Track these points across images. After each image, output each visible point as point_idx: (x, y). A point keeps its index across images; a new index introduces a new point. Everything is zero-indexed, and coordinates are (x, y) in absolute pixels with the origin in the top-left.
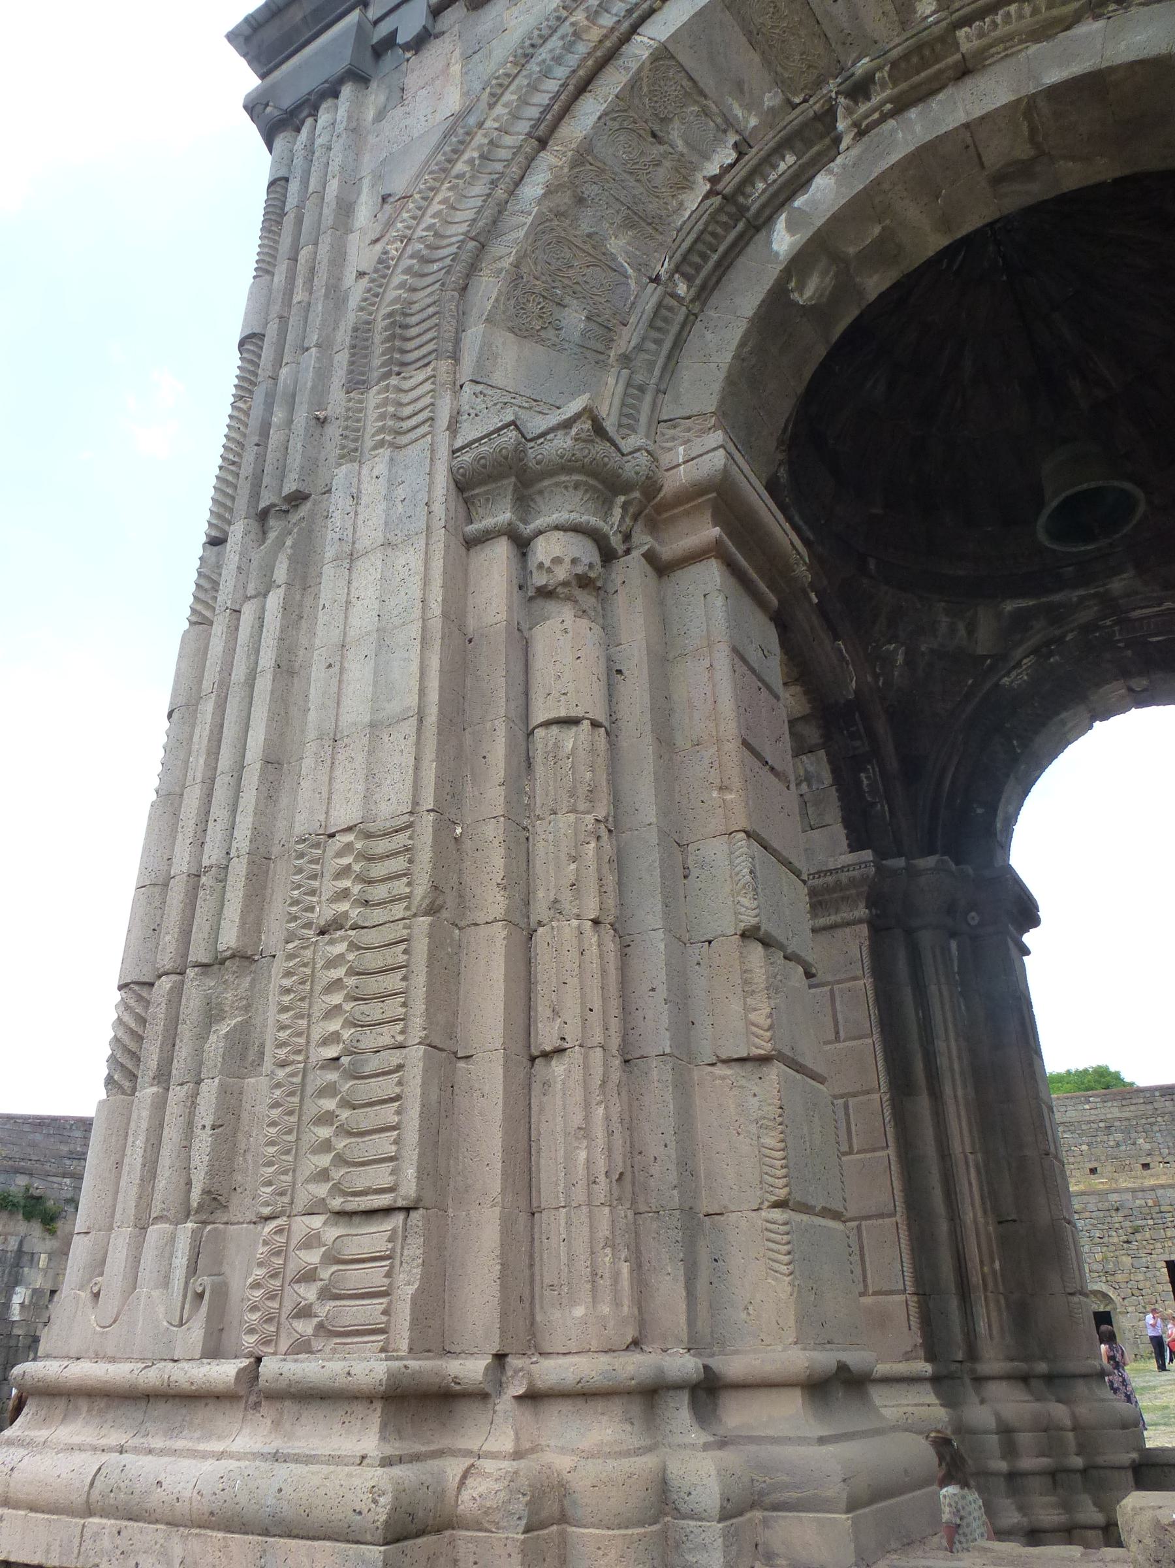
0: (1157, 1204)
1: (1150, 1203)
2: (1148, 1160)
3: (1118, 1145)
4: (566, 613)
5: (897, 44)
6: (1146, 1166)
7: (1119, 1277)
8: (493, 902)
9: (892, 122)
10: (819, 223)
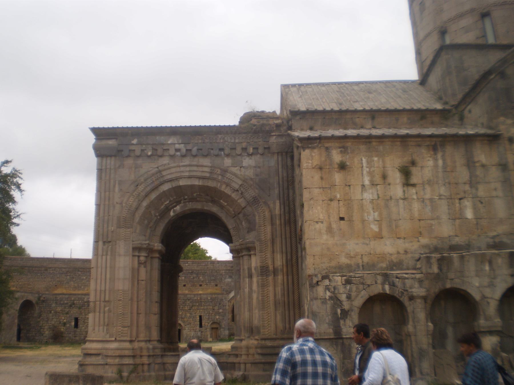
0: (201, 299)
1: (199, 299)
2: (202, 283)
3: (194, 278)
4: (143, 266)
6: (201, 285)
7: (185, 319)
8: (135, 299)
9: (187, 203)
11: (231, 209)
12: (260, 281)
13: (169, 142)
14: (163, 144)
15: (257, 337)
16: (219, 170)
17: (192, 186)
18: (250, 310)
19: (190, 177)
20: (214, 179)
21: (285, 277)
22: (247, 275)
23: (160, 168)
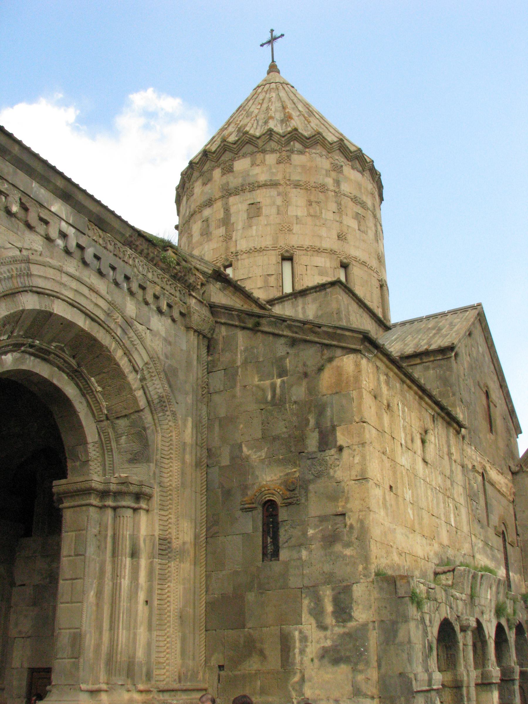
5: (45, 346)
10: (5, 370)
11: (104, 404)
12: (159, 567)
13: (53, 209)
14: (42, 205)
15: (141, 687)
16: (120, 317)
17: (70, 325)
18: (132, 627)
19: (72, 304)
20: (108, 330)
21: (192, 567)
22: (128, 551)
23: (25, 253)
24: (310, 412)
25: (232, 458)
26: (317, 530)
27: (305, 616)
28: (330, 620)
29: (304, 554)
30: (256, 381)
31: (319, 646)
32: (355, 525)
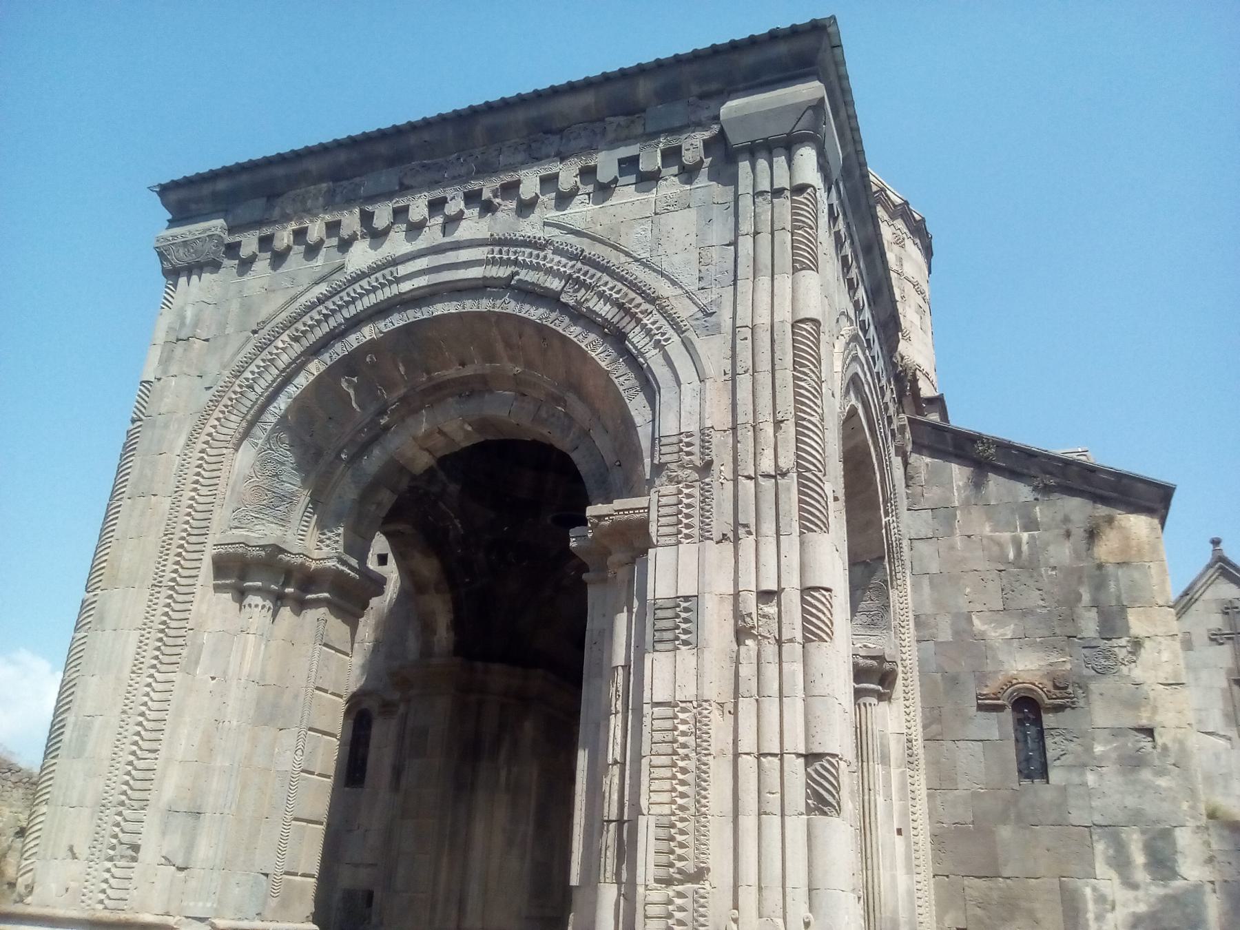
24: (1080, 581)
25: (956, 633)
26: (1109, 747)
27: (1101, 868)
28: (1141, 876)
29: (1091, 778)
30: (987, 530)
31: (1126, 911)
32: (1170, 745)
